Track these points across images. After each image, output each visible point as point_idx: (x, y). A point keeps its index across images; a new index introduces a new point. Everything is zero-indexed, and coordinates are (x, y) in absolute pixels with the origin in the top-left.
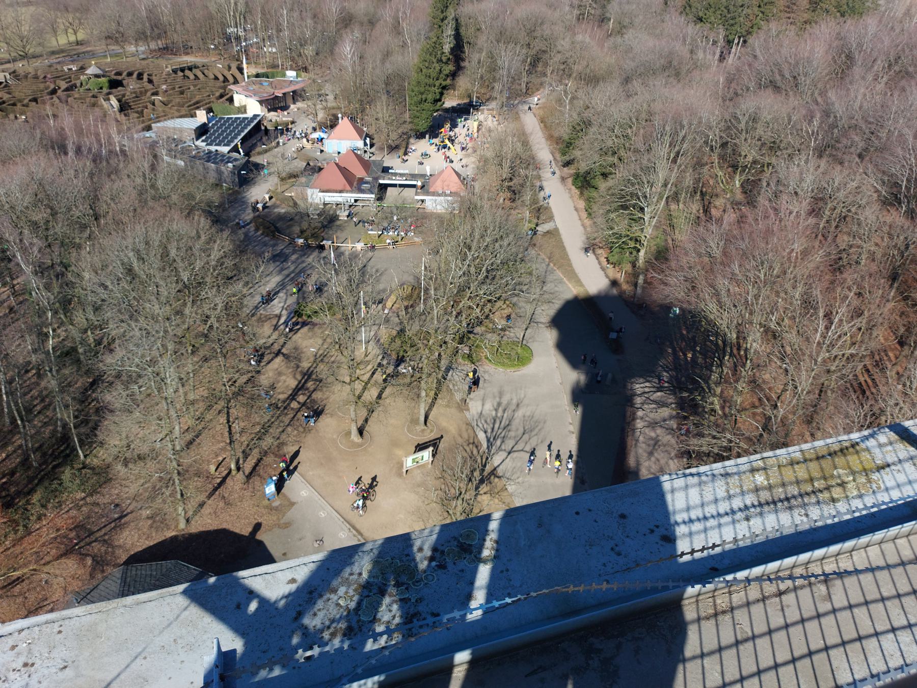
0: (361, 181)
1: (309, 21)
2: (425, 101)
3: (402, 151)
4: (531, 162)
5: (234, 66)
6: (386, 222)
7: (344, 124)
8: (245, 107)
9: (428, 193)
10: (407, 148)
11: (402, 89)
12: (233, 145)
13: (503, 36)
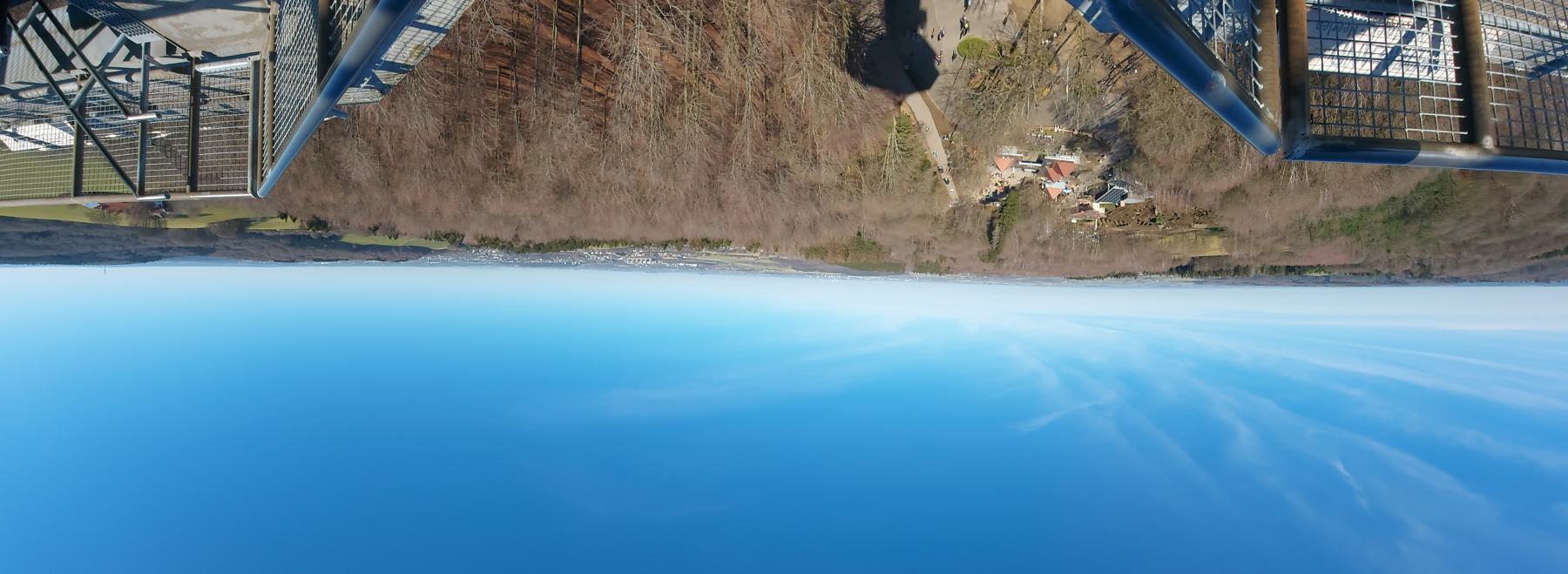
0: (1051, 166)
4: (956, 175)
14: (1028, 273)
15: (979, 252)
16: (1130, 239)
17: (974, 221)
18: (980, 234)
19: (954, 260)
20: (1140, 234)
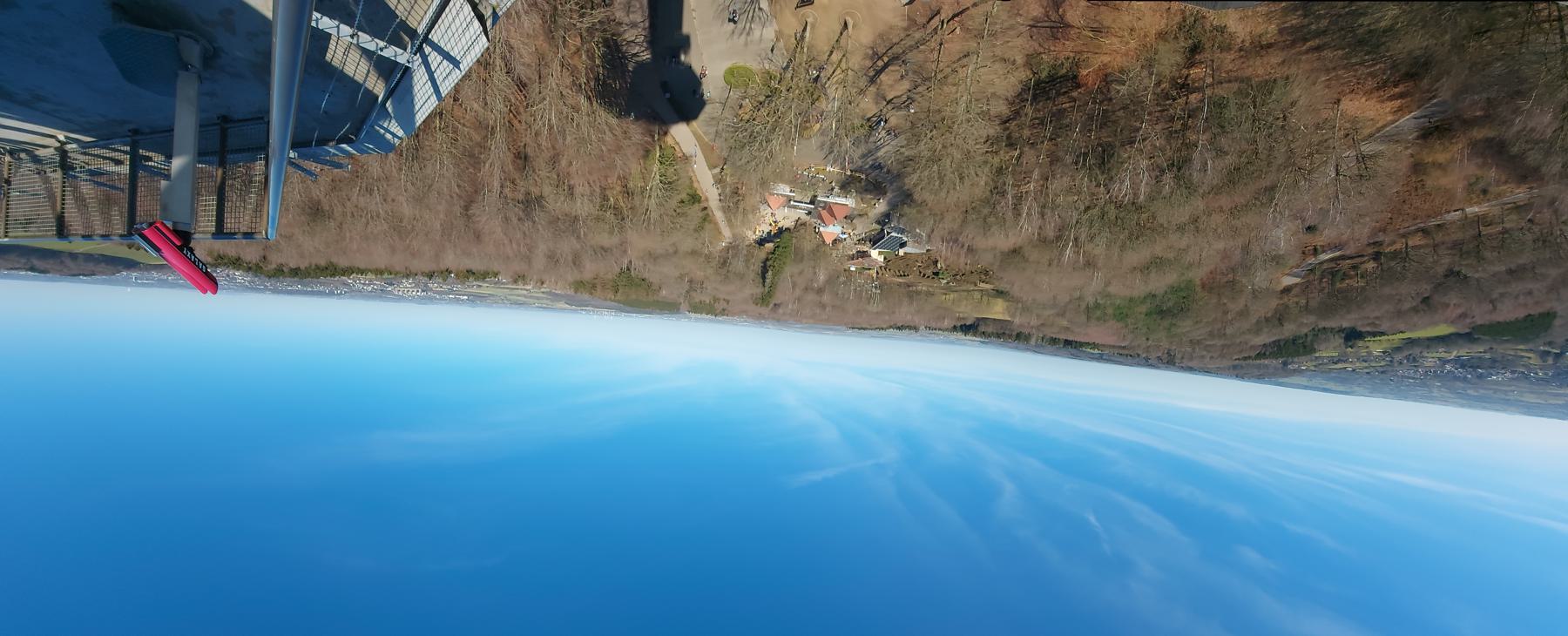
0: (824, 208)
1: (840, 292)
5: (880, 274)
6: (813, 183)
7: (829, 241)
9: (788, 196)
11: (796, 254)
13: (741, 276)
14: (804, 321)
16: (911, 291)
17: (747, 261)
18: (752, 275)
20: (923, 286)
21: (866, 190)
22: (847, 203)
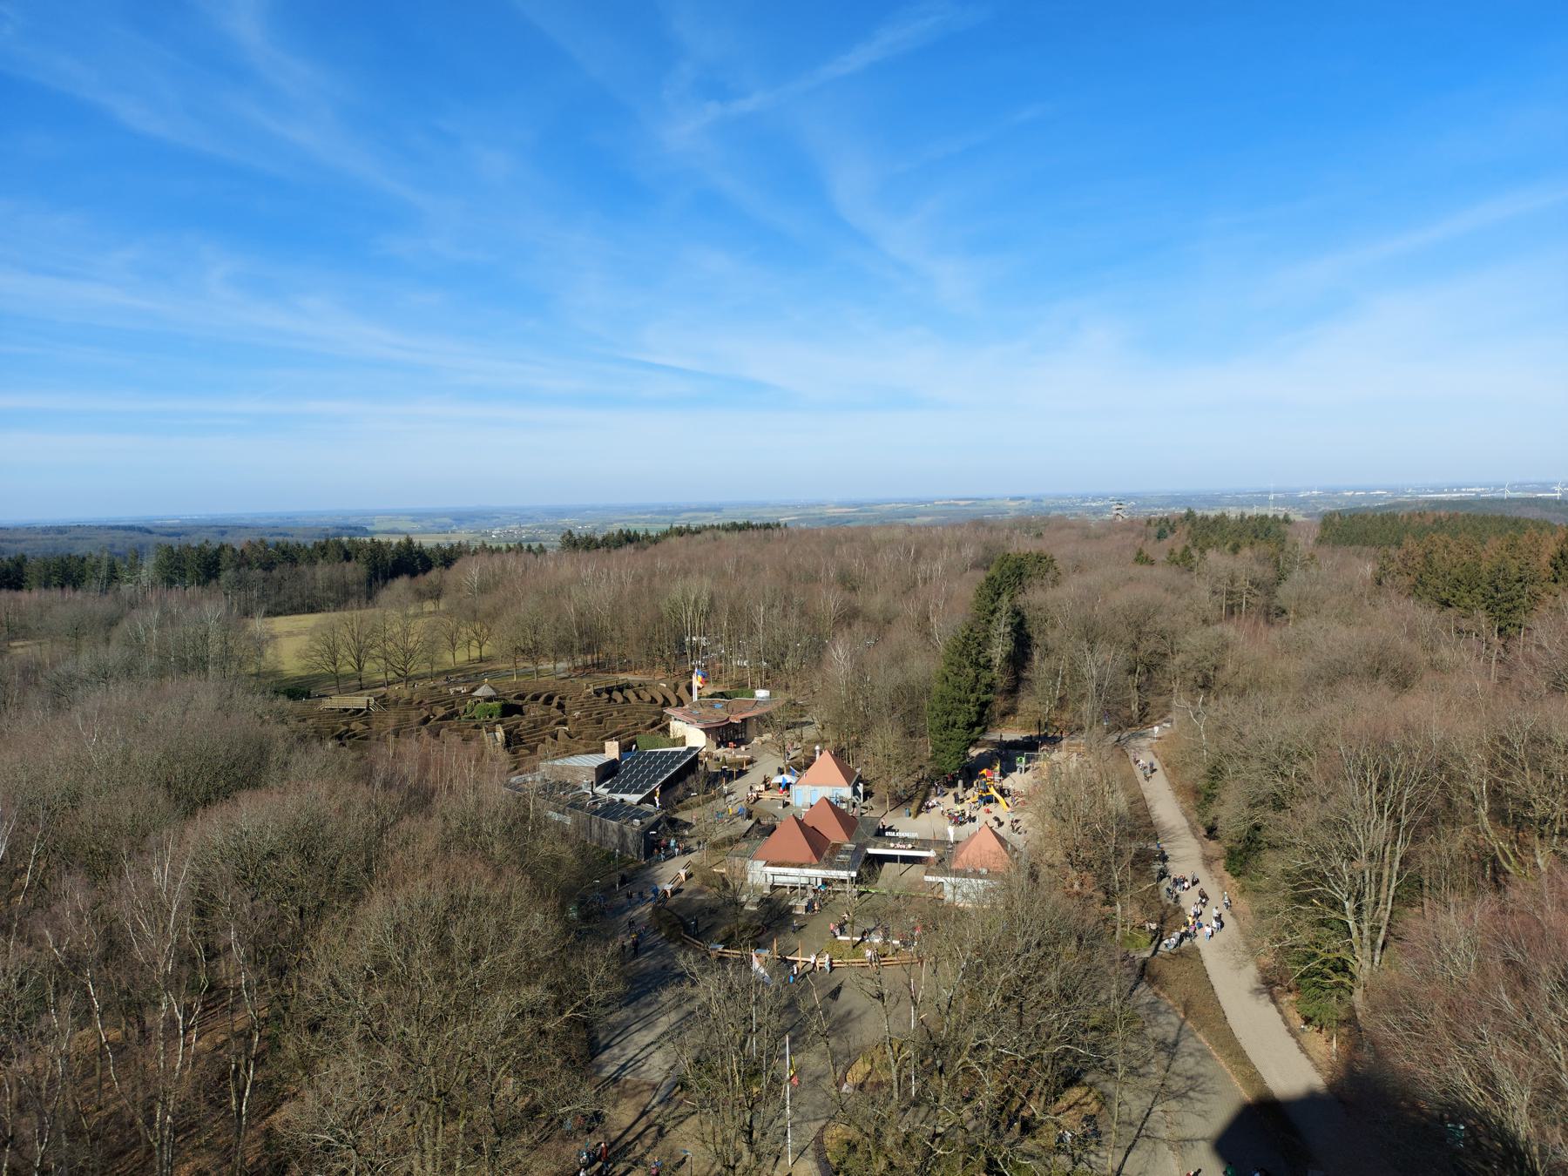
0: (837, 848)
2: (955, 723)
3: (916, 804)
4: (1141, 824)
8: (684, 738)
9: (947, 872)
10: (926, 798)
12: (648, 791)
13: (1091, 634)
15: (1055, 583)
16: (588, 649)
18: (1053, 637)
19: (1142, 559)
20: (554, 670)
21: (713, 911)
22: (770, 869)
